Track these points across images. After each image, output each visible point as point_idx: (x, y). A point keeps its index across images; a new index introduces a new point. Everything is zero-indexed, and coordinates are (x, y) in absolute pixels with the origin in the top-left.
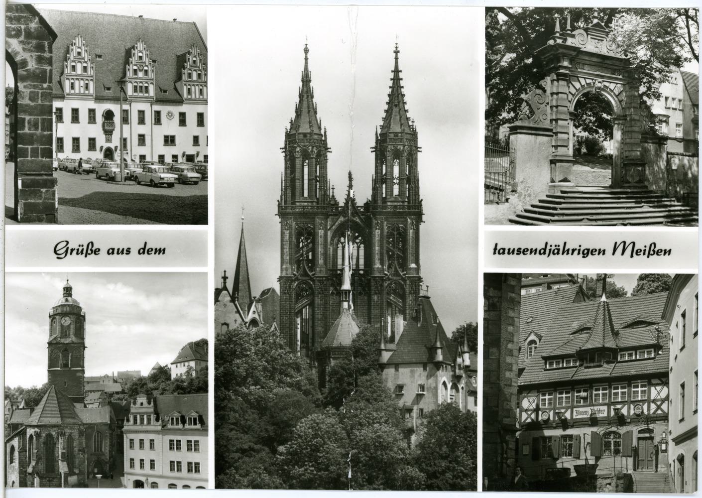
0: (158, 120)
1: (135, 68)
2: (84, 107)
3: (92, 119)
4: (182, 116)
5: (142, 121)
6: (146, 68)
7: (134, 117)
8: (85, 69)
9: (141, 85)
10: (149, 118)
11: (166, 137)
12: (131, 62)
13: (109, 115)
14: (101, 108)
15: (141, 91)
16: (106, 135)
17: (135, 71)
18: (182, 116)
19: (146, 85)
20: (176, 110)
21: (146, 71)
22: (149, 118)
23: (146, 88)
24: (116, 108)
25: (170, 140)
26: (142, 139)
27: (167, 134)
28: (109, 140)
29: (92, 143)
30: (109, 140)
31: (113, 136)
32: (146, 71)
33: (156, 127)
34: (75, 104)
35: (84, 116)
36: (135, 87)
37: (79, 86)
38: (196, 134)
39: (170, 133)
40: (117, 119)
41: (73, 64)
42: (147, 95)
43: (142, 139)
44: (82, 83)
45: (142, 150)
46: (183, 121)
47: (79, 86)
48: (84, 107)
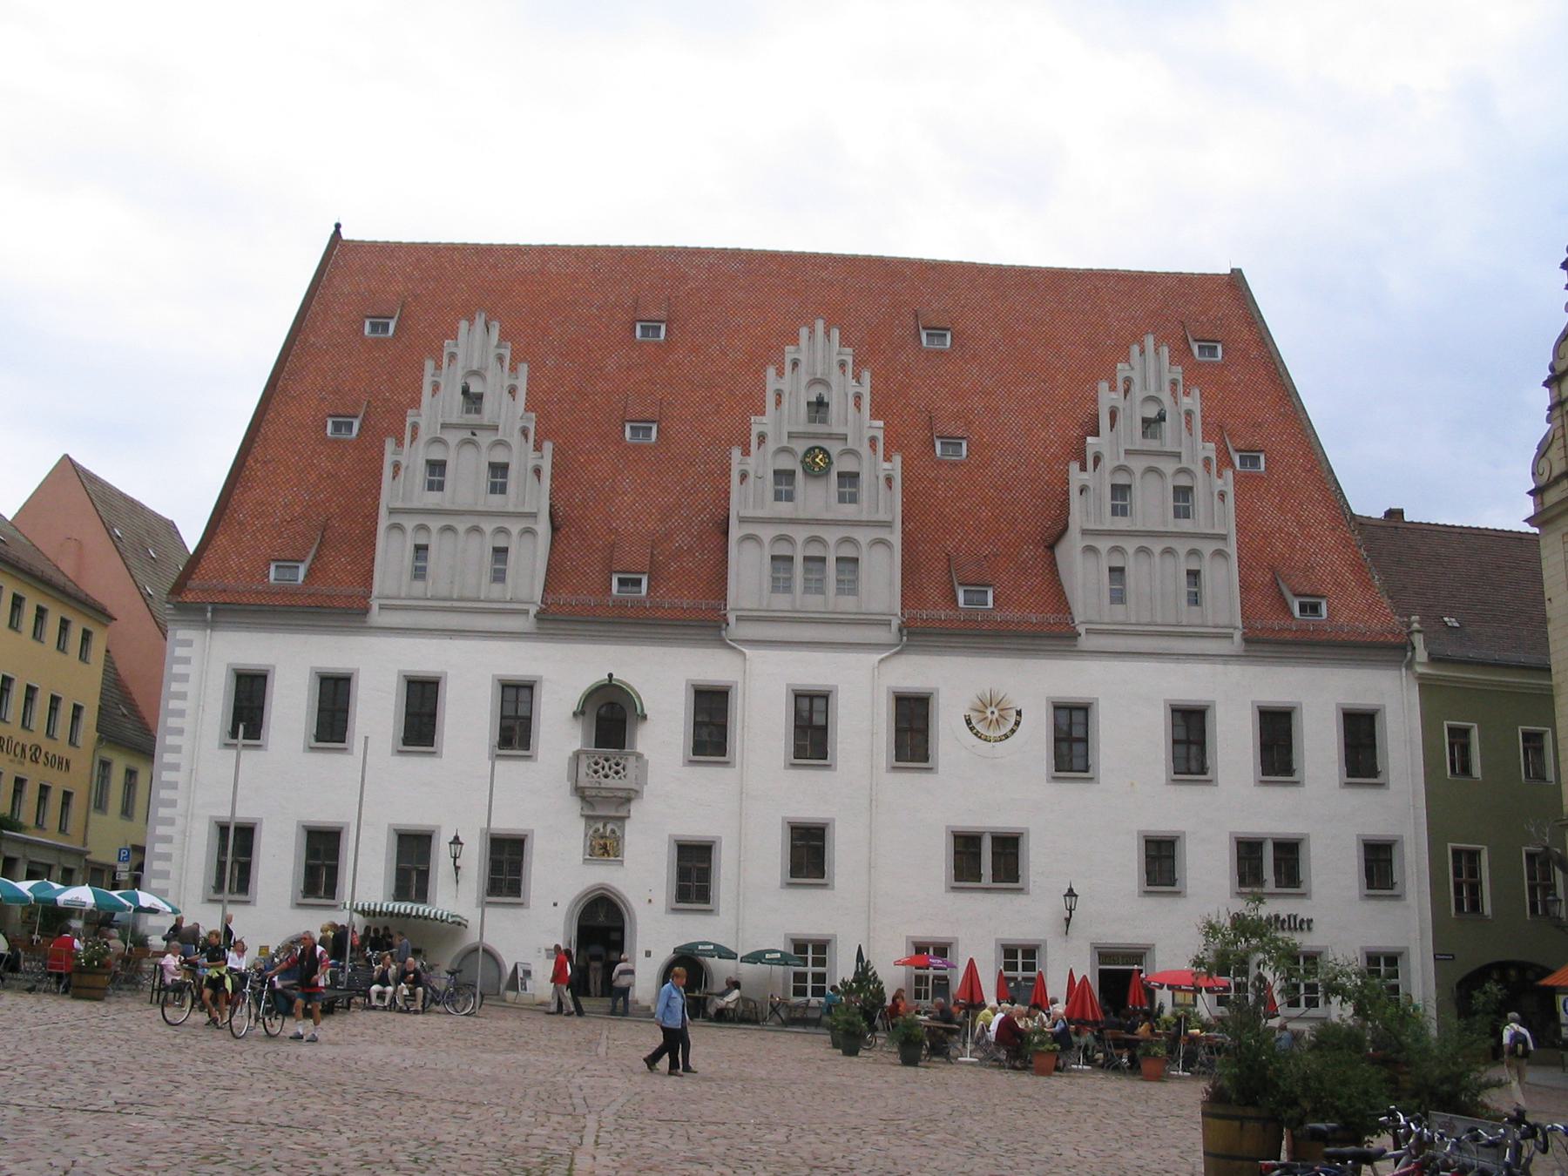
1: (786, 463)
6: (847, 465)
7: (762, 724)
9: (815, 551)
10: (862, 727)
11: (966, 847)
12: (762, 438)
13: (611, 716)
14: (566, 672)
15: (815, 586)
16: (588, 818)
17: (784, 476)
19: (847, 552)
20: (1034, 683)
21: (849, 478)
22: (862, 727)
24: (662, 677)
25: (989, 859)
26: (808, 851)
27: (969, 822)
28: (605, 847)
29: (506, 863)
30: (605, 847)
31: (628, 825)
32: (849, 478)
34: (423, 656)
35: (468, 717)
36: (781, 561)
37: (459, 562)
38: (1161, 826)
39: (990, 819)
40: (663, 732)
41: (437, 454)
42: (848, 604)
43: (808, 851)
44: (478, 551)
45: (807, 913)
47: (459, 562)
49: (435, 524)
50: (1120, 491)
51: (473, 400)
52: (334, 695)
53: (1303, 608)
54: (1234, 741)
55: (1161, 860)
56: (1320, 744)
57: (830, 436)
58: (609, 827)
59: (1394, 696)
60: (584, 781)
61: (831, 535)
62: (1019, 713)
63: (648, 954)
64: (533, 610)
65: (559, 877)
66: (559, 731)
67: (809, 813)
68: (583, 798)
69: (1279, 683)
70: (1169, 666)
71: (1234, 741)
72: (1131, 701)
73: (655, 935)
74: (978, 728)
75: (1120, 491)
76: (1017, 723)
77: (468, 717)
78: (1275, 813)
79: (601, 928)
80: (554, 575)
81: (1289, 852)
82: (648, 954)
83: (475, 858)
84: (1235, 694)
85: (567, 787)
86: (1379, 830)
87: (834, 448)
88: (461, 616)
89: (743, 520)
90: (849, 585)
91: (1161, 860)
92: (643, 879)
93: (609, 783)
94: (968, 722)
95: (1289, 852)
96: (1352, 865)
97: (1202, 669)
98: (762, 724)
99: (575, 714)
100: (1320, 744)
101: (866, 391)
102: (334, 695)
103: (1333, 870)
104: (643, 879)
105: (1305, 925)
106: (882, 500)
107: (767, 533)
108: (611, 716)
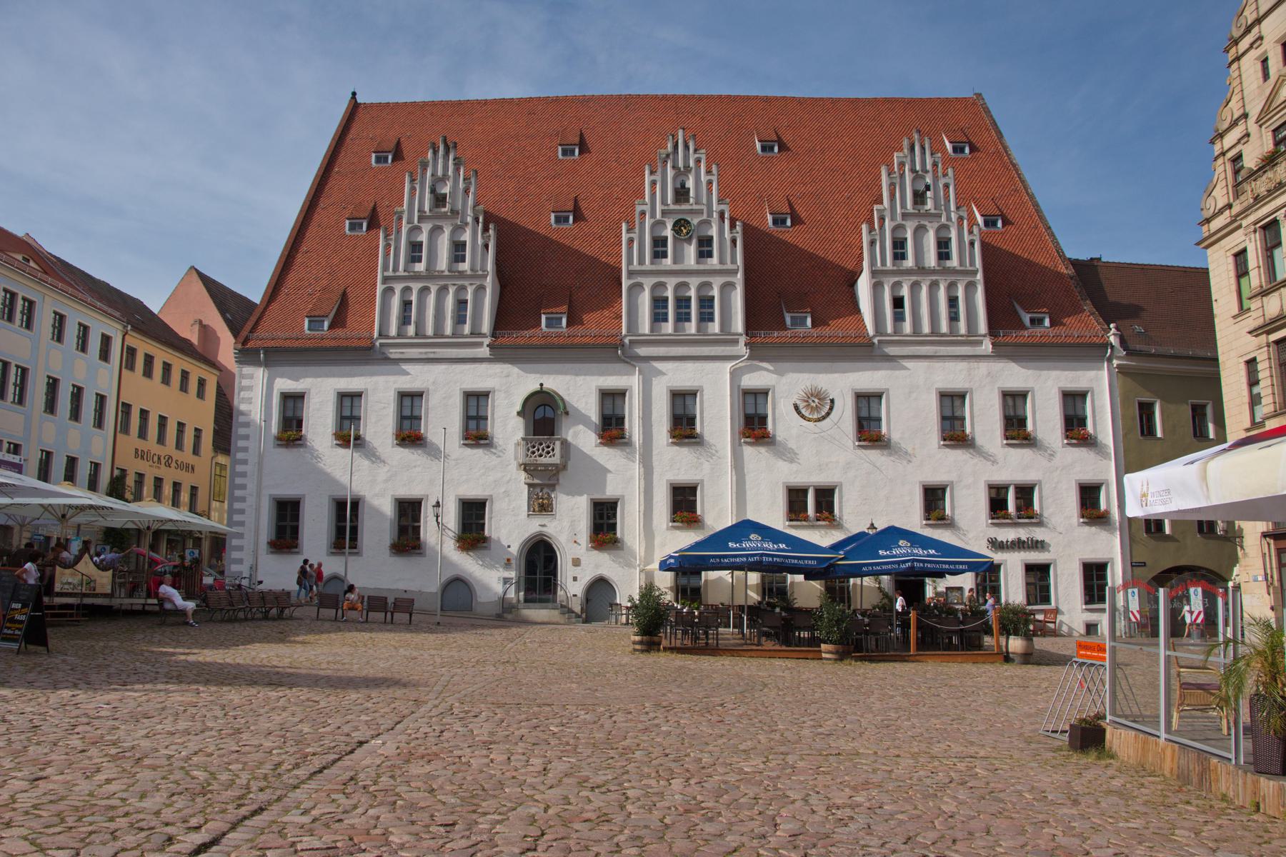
0: (754, 426)
2: (442, 386)
3: (476, 433)
4: (867, 402)
5: (684, 427)
8: (458, 249)
10: (718, 417)
14: (511, 386)
16: (530, 485)
17: (659, 242)
18: (867, 402)
22: (718, 417)
23: (706, 302)
26: (684, 502)
27: (799, 480)
28: (542, 506)
30: (542, 506)
33: (754, 455)
35: (443, 421)
36: (659, 303)
37: (435, 309)
39: (810, 475)
46: (869, 431)
47: (435, 309)
48: (442, 386)
49: (416, 286)
50: (899, 244)
51: (439, 200)
52: (349, 405)
53: (1032, 321)
54: (985, 419)
55: (933, 498)
56: (1045, 417)
57: (692, 212)
58: (545, 490)
59: (1099, 383)
60: (528, 460)
61: (694, 282)
62: (832, 401)
63: (575, 579)
64: (487, 341)
65: (511, 526)
66: (508, 426)
67: (684, 477)
68: (525, 470)
69: (1014, 375)
70: (937, 365)
71: (985, 419)
72: (910, 393)
73: (579, 567)
74: (803, 411)
75: (899, 244)
76: (831, 409)
77: (443, 421)
78: (1014, 466)
79: (540, 562)
80: (502, 321)
81: (1025, 493)
82: (575, 579)
83: (451, 517)
84: (987, 381)
85: (514, 465)
86: (1089, 477)
87: (695, 221)
88: (436, 348)
89: (631, 274)
90: (706, 317)
91: (933, 498)
92: (569, 524)
93: (544, 460)
94: (796, 408)
95: (1025, 493)
96: (1072, 501)
97: (962, 365)
98: (648, 414)
99: (519, 413)
100: (1045, 417)
101: (715, 178)
102: (349, 405)
103: (1059, 505)
104: (569, 524)
105: (1038, 545)
106: (730, 257)
107: (648, 282)
108: (543, 415)
